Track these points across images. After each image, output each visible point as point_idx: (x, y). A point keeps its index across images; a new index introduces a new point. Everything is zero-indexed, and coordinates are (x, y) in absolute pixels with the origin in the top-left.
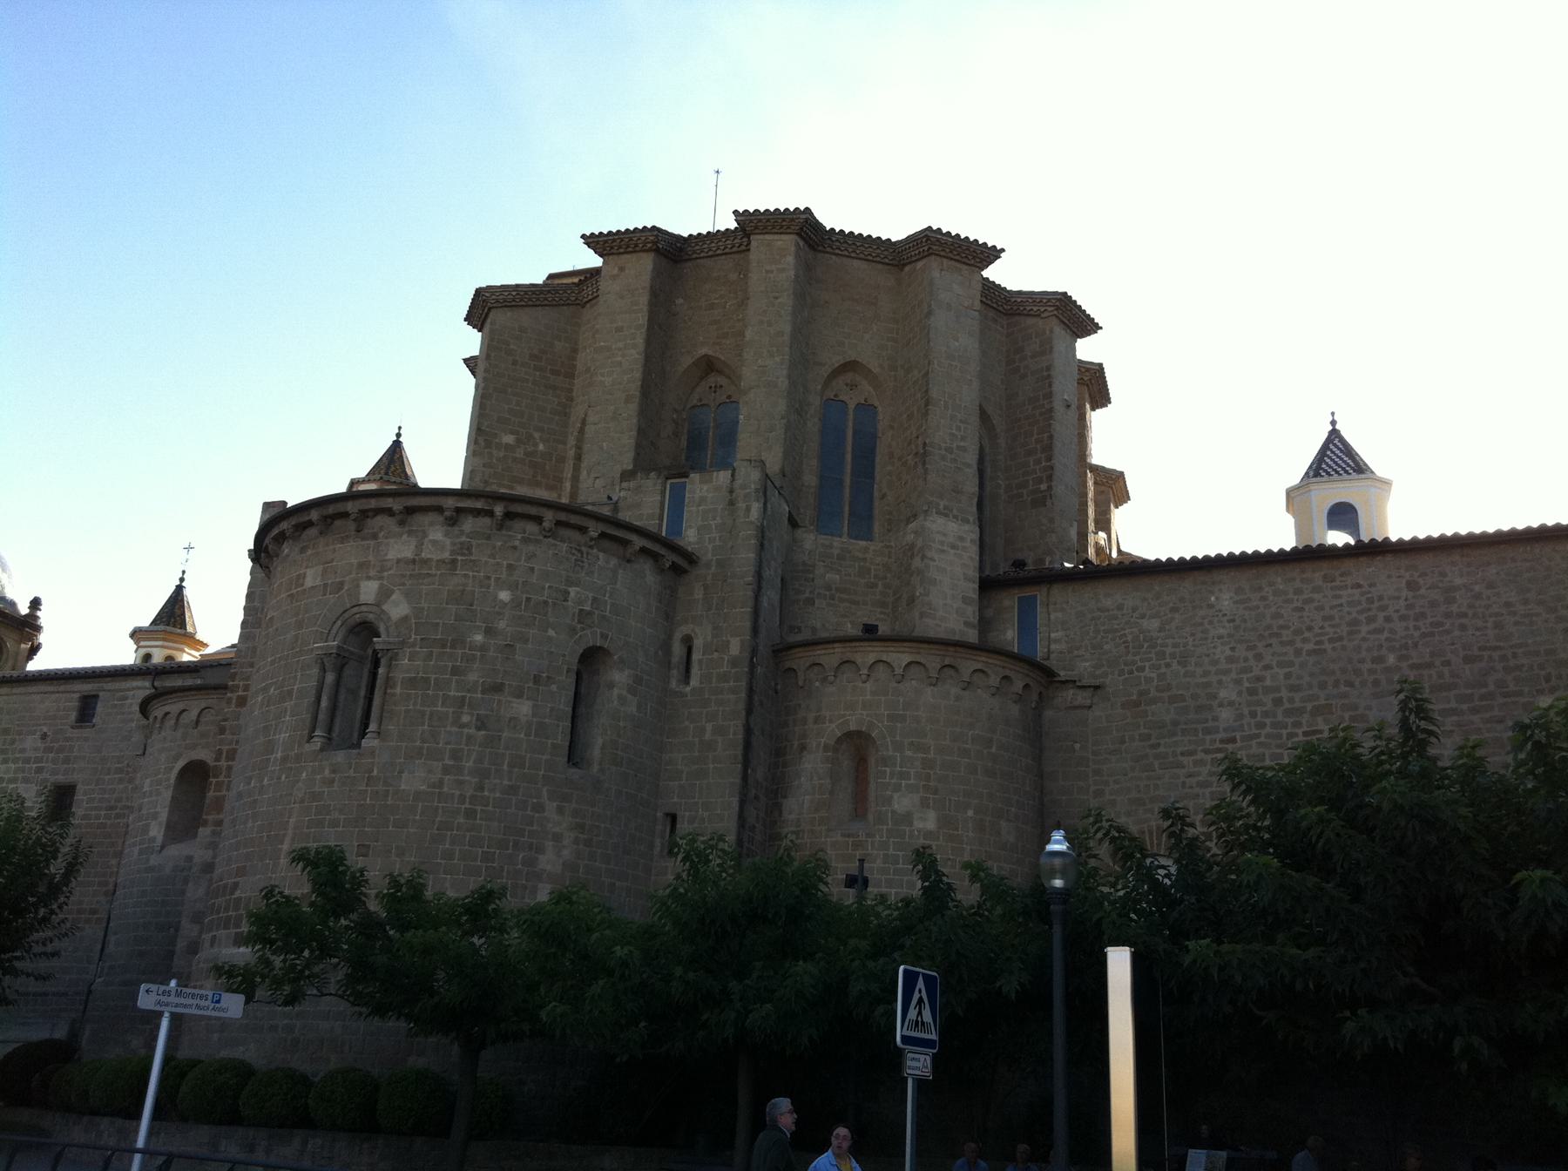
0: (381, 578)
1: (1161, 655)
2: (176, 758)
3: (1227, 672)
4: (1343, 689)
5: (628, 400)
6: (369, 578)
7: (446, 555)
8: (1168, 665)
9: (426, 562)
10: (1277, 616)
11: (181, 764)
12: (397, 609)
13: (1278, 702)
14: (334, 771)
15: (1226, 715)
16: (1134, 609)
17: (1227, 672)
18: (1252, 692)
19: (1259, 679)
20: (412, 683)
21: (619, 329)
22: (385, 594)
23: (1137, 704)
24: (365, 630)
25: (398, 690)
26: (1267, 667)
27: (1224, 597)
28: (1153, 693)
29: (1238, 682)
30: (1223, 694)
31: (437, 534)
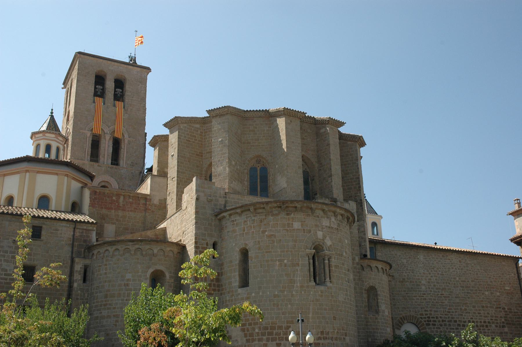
0: (323, 231)
1: (407, 269)
2: (149, 268)
3: (423, 276)
4: (448, 284)
5: (299, 167)
6: (319, 230)
7: (336, 227)
8: (409, 273)
9: (332, 228)
10: (433, 264)
11: (151, 271)
12: (328, 242)
13: (435, 285)
14: (322, 293)
15: (423, 287)
16: (400, 256)
17: (423, 276)
18: (429, 282)
19: (430, 279)
20: (336, 266)
21: (293, 142)
22: (324, 237)
23: (402, 282)
24: (318, 248)
25: (333, 268)
26: (432, 276)
27: (421, 257)
28: (406, 280)
29: (426, 279)
30: (422, 282)
31: (333, 219)
